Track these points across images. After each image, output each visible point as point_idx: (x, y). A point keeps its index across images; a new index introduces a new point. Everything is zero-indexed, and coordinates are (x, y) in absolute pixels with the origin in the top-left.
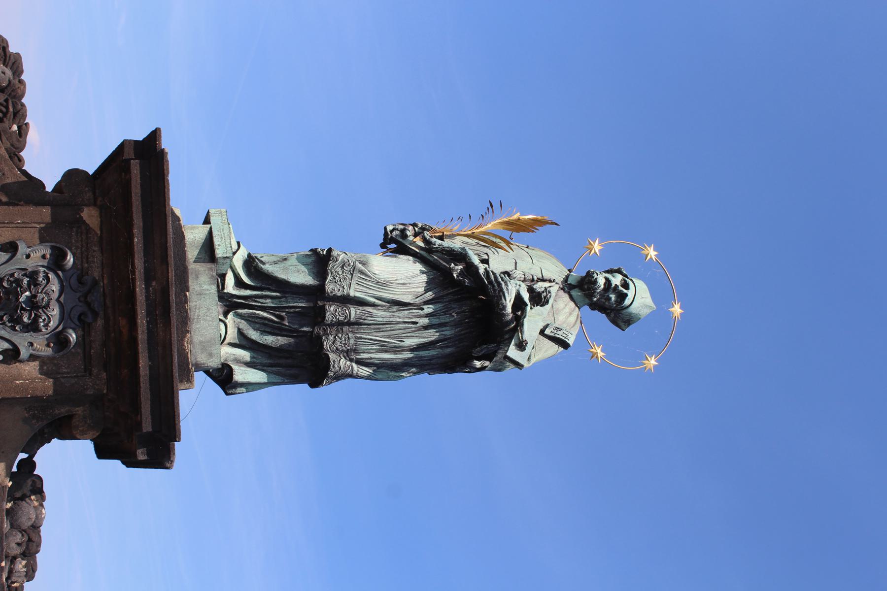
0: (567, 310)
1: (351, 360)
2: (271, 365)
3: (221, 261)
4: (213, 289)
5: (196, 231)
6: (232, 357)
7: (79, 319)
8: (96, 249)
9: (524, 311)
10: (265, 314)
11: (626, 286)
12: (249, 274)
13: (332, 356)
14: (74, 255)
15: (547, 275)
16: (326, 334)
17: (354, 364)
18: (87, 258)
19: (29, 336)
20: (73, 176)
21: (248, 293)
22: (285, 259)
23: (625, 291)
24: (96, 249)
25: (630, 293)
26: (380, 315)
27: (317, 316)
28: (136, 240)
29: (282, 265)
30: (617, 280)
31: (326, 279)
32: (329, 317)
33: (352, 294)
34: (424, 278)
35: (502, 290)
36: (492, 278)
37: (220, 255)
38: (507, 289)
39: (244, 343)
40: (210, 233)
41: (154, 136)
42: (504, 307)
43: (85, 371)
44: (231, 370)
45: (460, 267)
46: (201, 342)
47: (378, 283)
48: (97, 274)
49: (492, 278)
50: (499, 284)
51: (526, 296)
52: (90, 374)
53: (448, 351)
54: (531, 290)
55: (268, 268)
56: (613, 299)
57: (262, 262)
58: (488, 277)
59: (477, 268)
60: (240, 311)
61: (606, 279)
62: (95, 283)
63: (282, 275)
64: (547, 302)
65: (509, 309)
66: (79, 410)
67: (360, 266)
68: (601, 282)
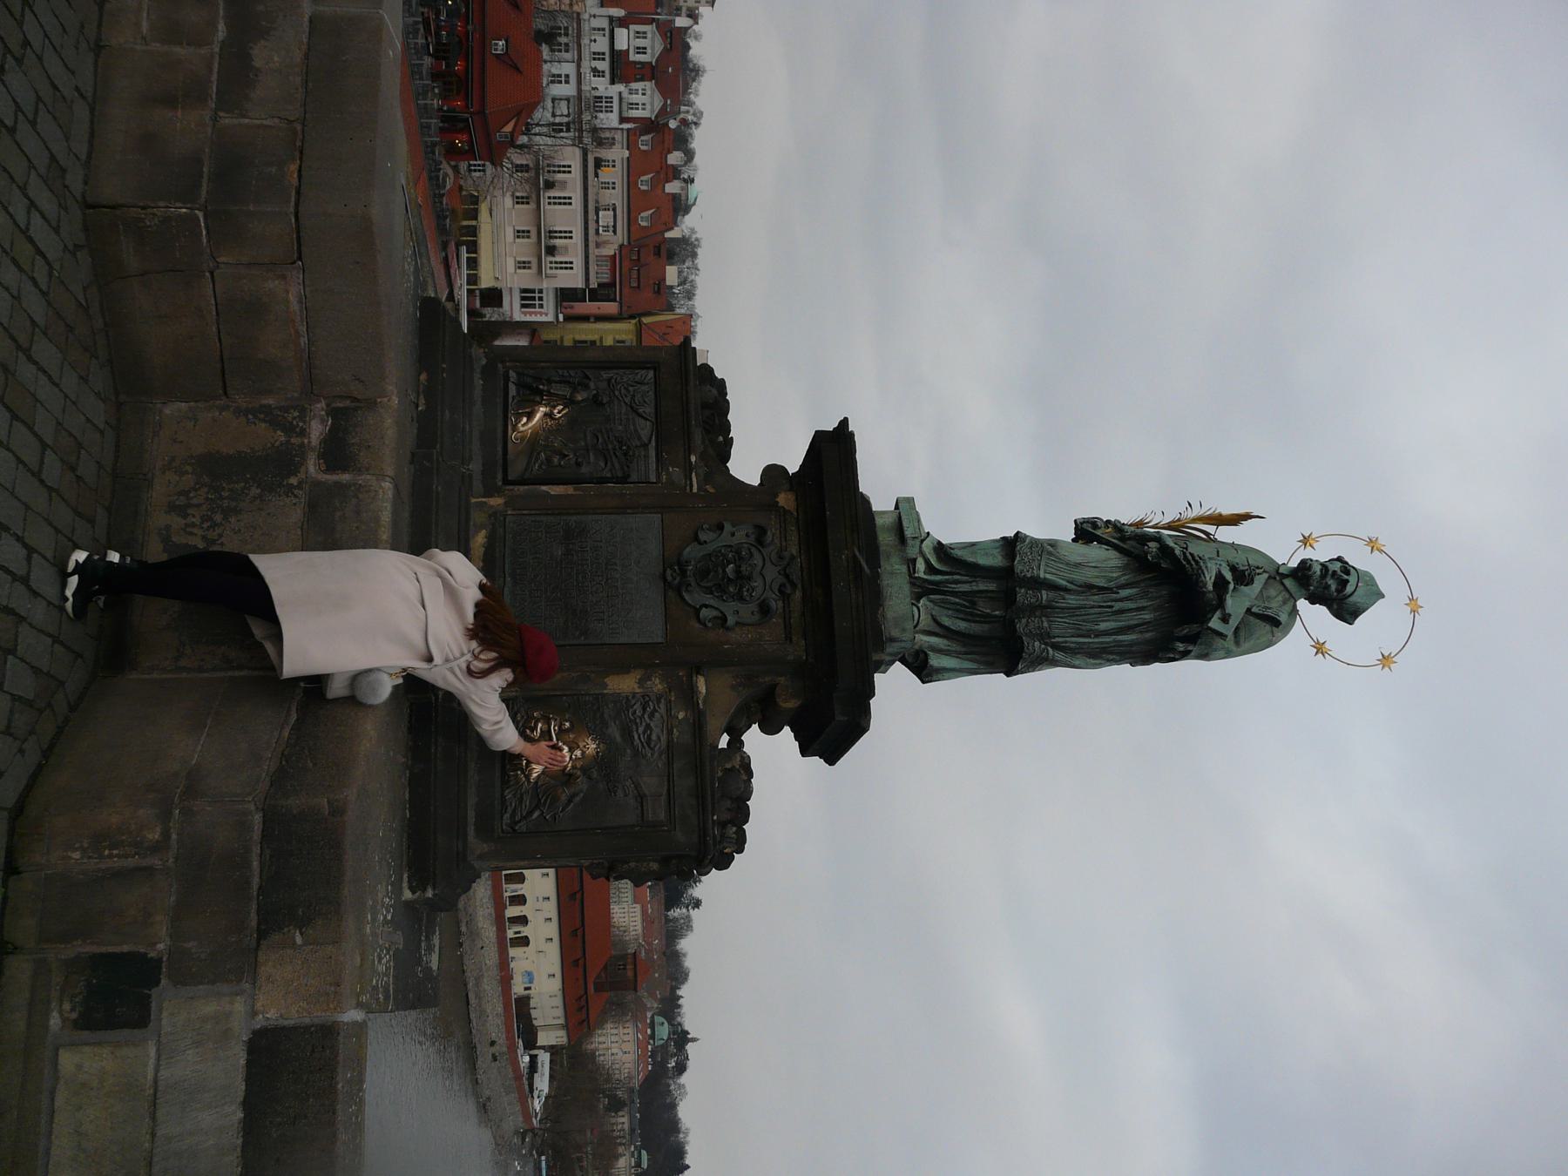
3: (910, 542)
4: (904, 569)
7: (780, 591)
9: (1226, 590)
11: (1348, 573)
12: (939, 559)
19: (734, 605)
20: (773, 473)
25: (1352, 579)
26: (1072, 600)
27: (1008, 598)
30: (1337, 566)
39: (937, 630)
40: (900, 518)
41: (844, 423)
42: (1205, 585)
44: (926, 655)
48: (794, 552)
51: (1228, 576)
53: (1148, 635)
54: (1233, 569)
55: (958, 553)
56: (1333, 587)
62: (793, 558)
64: (1251, 582)
65: (1210, 587)
66: (782, 680)
68: (1317, 569)
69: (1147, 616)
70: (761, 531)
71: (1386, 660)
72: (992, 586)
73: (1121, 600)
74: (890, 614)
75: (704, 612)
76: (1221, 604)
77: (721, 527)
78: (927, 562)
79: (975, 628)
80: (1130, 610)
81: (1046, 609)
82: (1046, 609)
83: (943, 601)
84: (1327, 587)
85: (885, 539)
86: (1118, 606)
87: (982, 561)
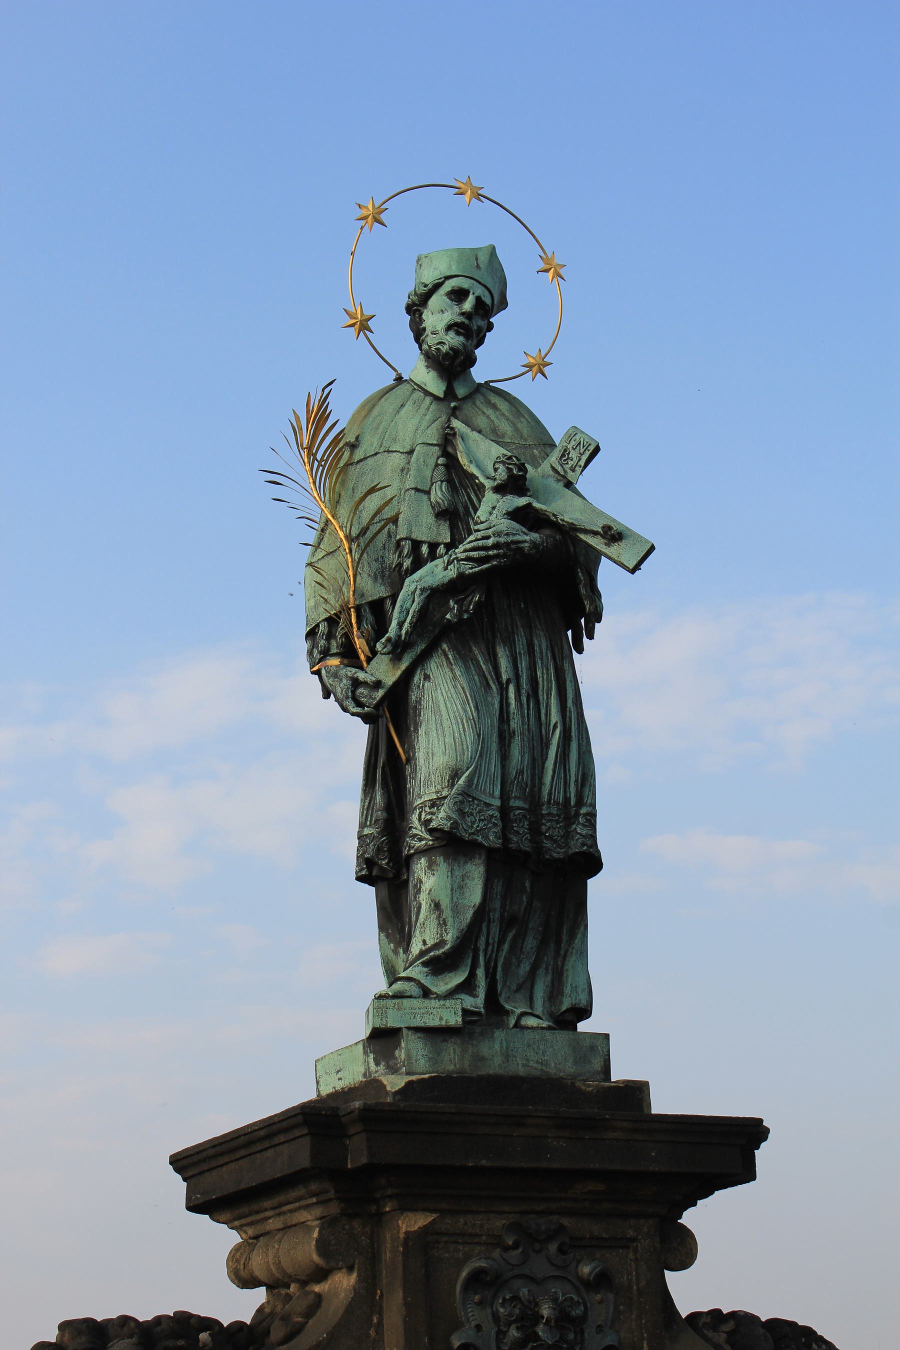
0: (489, 412)
1: (577, 814)
2: (558, 942)
5: (414, 1053)
6: (547, 1005)
8: (462, 1221)
10: (506, 947)
11: (459, 295)
13: (576, 846)
14: (467, 1258)
15: (433, 435)
16: (539, 849)
17: (583, 811)
18: (476, 1235)
21: (480, 973)
22: (437, 906)
23: (471, 299)
24: (462, 1221)
28: (484, 1162)
29: (447, 913)
31: (480, 845)
32: (526, 846)
33: (497, 803)
35: (507, 544)
36: (482, 553)
37: (460, 1019)
38: (507, 534)
40: (417, 1030)
42: (534, 544)
43: (627, 1247)
45: (451, 603)
46: (575, 1063)
47: (481, 756)
49: (482, 553)
50: (496, 546)
52: (633, 1240)
54: (500, 489)
57: (436, 946)
58: (480, 561)
59: (461, 576)
60: (499, 987)
61: (449, 328)
63: (469, 914)
64: (522, 468)
65: (535, 536)
67: (462, 781)
68: (453, 340)
69: (541, 643)
72: (498, 887)
73: (517, 677)
74: (570, 1068)
79: (535, 922)
80: (532, 668)
83: (503, 970)
84: (480, 329)
85: (453, 1059)
87: (475, 895)
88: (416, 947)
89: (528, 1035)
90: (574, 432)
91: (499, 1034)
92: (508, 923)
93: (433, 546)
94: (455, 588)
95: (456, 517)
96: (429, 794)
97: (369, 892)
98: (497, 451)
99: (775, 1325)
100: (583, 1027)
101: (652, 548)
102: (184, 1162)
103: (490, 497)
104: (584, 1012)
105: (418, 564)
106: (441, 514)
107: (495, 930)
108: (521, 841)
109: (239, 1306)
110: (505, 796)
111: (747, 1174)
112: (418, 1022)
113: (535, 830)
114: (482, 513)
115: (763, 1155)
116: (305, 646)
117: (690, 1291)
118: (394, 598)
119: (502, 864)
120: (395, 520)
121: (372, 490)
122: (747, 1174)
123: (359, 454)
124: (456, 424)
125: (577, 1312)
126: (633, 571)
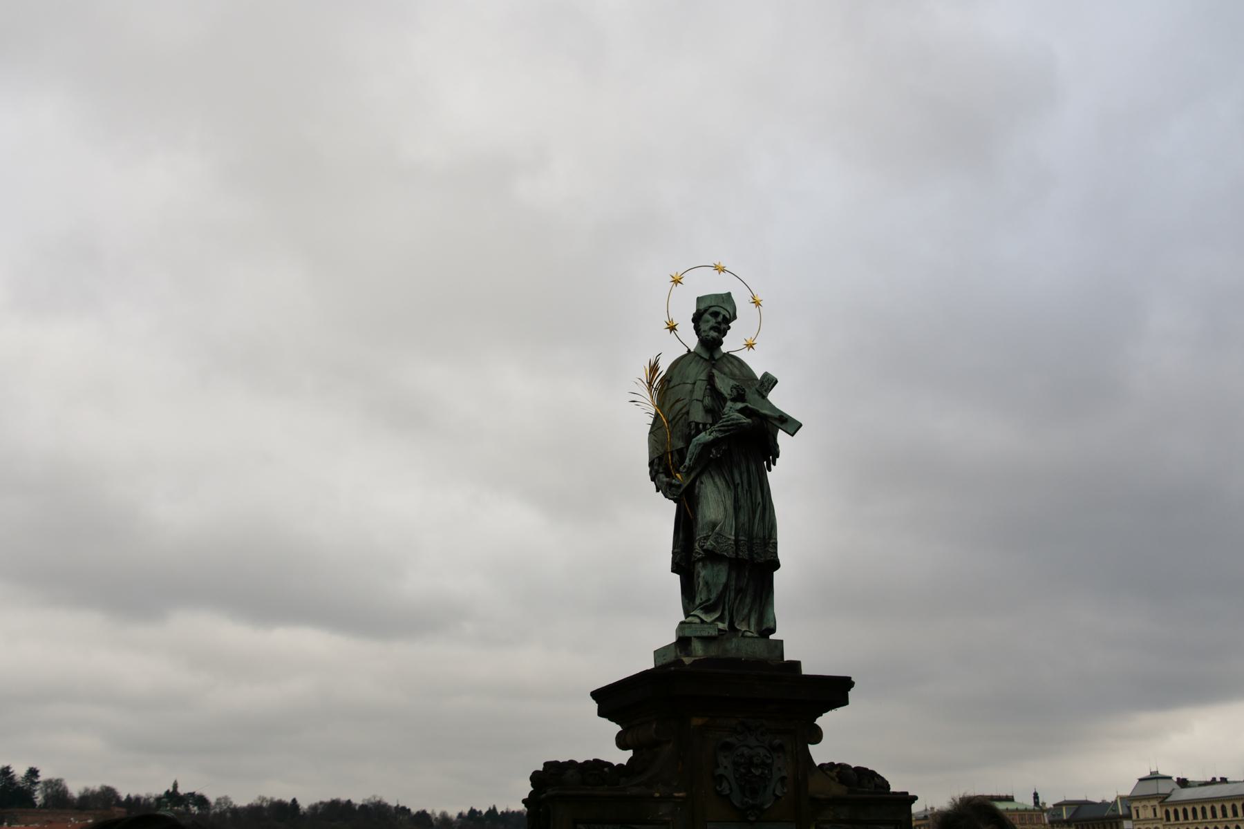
11: (716, 314)
21: (726, 613)
26: (743, 518)
32: (746, 557)
34: (717, 480)
40: (698, 638)
51: (740, 405)
54: (734, 400)
55: (714, 596)
58: (725, 431)
63: (721, 588)
64: (743, 390)
65: (749, 420)
68: (714, 334)
70: (727, 747)
71: (757, 303)
72: (734, 575)
75: (778, 793)
76: (765, 417)
77: (721, 776)
78: (717, 620)
81: (751, 538)
82: (751, 538)
85: (714, 651)
86: (746, 486)
87: (723, 579)
88: (698, 601)
89: (747, 640)
90: (766, 375)
91: (734, 640)
92: (740, 591)
93: (705, 425)
94: (715, 443)
95: (714, 412)
96: (703, 534)
97: (677, 577)
98: (732, 383)
99: (858, 769)
100: (772, 637)
101: (801, 425)
102: (597, 695)
103: (729, 404)
104: (773, 631)
105: (698, 432)
106: (708, 411)
107: (733, 594)
108: (744, 554)
109: (622, 757)
110: (736, 535)
111: (844, 702)
112: (698, 634)
113: (750, 550)
114: (726, 410)
115: (852, 694)
116: (648, 469)
117: (820, 754)
118: (687, 447)
119: (736, 564)
120: (688, 413)
121: (678, 401)
122: (844, 702)
123: (672, 384)
124: (714, 371)
125: (769, 761)
126: (792, 435)
